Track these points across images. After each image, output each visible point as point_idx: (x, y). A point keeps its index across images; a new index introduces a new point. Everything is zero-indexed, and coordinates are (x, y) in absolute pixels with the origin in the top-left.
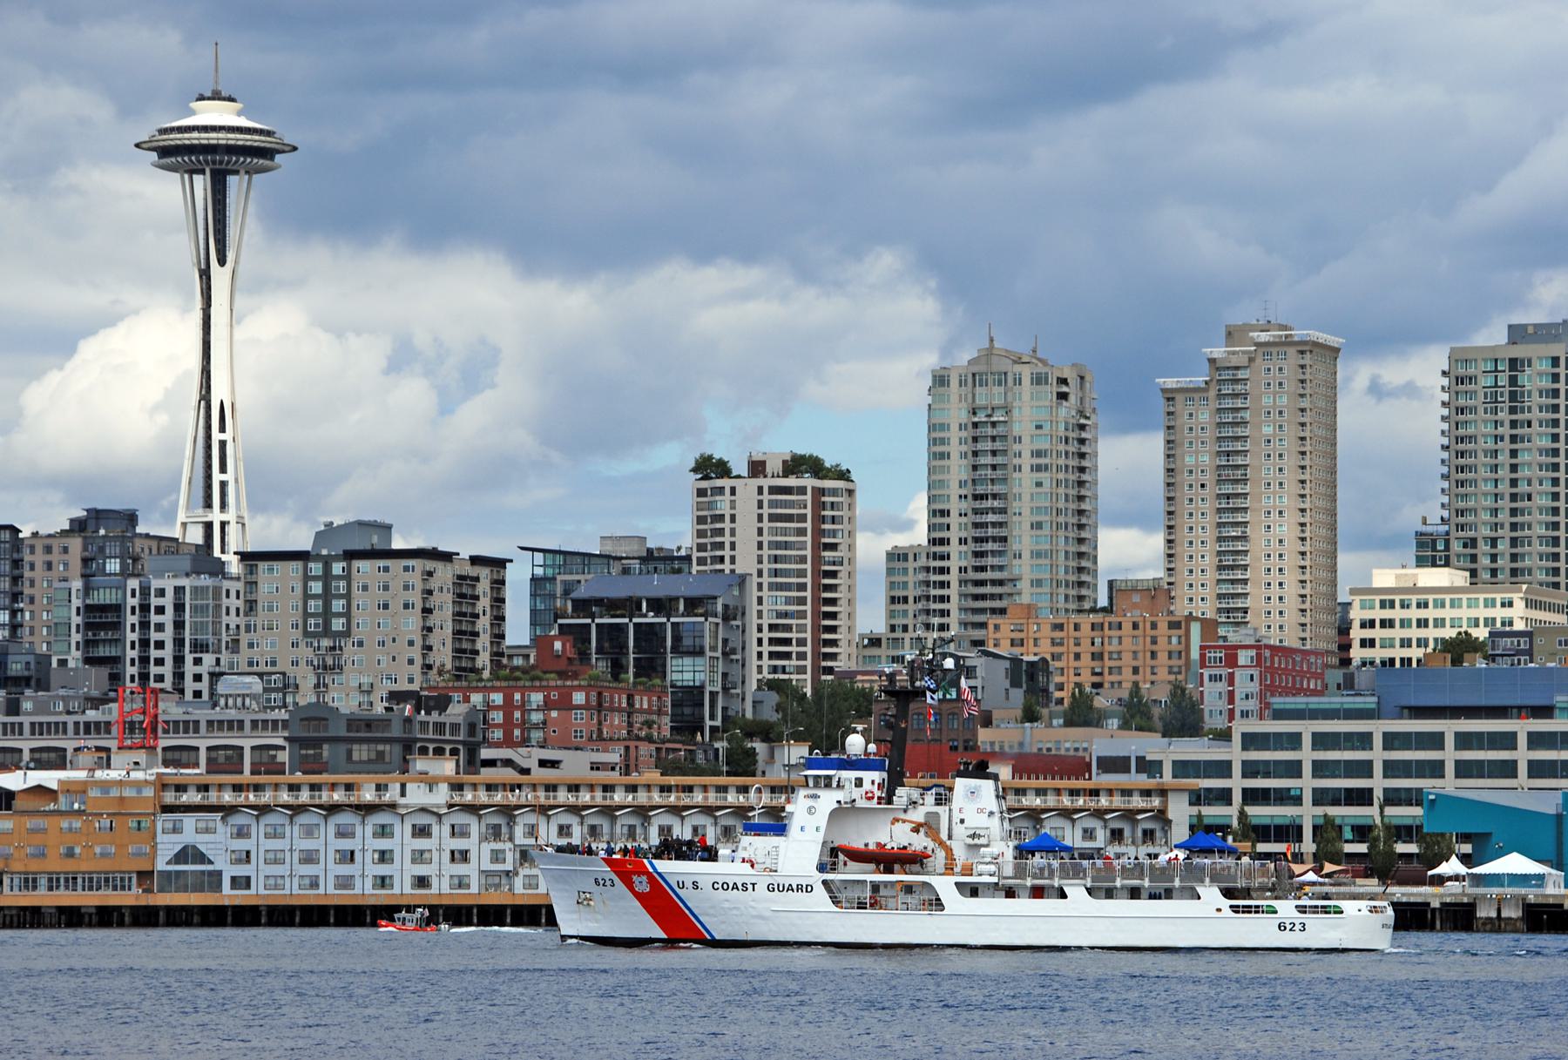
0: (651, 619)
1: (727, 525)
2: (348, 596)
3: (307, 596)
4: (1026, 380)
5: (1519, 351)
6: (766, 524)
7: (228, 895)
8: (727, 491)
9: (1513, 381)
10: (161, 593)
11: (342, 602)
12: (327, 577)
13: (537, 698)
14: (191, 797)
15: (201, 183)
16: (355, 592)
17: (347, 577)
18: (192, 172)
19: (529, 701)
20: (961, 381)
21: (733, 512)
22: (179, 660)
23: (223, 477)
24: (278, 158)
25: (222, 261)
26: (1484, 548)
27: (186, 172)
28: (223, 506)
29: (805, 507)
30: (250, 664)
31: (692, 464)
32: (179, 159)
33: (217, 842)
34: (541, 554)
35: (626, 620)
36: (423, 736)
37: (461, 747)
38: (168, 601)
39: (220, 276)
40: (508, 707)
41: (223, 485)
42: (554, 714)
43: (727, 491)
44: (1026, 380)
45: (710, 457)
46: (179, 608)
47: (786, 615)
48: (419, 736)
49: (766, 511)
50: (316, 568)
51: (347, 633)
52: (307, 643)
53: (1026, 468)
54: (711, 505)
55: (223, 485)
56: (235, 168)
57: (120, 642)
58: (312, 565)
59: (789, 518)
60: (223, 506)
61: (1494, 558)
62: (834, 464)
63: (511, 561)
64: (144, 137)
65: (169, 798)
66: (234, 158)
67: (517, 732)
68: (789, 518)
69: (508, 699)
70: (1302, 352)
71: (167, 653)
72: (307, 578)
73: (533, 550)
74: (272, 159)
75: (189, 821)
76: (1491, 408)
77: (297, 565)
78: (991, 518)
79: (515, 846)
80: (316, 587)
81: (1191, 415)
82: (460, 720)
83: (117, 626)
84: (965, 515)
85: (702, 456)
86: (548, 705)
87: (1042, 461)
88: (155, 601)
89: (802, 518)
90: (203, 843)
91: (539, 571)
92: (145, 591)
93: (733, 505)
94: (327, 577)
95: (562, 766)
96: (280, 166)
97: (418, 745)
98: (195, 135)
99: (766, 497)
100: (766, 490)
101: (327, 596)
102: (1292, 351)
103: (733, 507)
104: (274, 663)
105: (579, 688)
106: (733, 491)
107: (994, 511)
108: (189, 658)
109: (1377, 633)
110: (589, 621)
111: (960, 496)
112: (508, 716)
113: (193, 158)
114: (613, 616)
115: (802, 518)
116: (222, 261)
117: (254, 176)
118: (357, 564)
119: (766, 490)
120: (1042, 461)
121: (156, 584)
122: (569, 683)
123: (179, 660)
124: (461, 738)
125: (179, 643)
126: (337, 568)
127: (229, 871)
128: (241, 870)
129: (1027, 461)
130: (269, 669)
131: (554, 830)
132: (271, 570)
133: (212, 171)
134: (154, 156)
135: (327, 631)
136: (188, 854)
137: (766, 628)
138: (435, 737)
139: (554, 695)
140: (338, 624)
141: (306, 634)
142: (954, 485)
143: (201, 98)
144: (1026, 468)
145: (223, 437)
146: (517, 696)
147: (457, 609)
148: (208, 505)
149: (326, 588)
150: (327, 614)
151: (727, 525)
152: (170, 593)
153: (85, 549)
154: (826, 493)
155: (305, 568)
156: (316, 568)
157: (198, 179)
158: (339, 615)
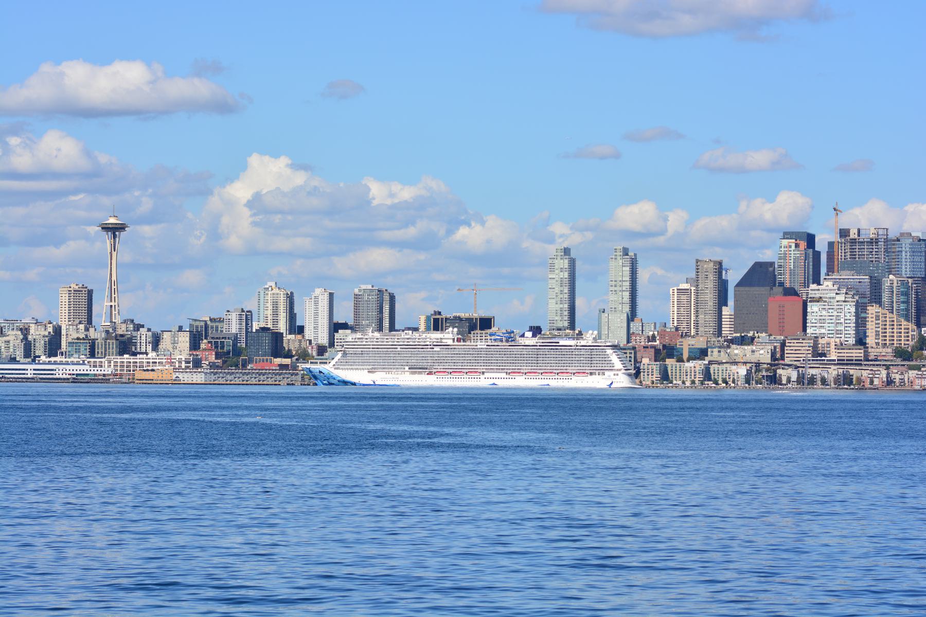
2: (178, 338)
6: (237, 321)
7: (182, 382)
14: (177, 370)
22: (146, 345)
24: (126, 229)
25: (115, 251)
28: (115, 301)
33: (181, 376)
39: (114, 254)
41: (115, 297)
50: (173, 333)
55: (115, 297)
60: (115, 301)
65: (175, 370)
71: (144, 344)
75: (177, 373)
86: (208, 355)
99: (237, 316)
108: (148, 345)
109: (339, 341)
116: (115, 251)
121: (142, 333)
123: (146, 345)
125: (146, 343)
127: (182, 379)
128: (184, 379)
136: (177, 377)
143: (110, 217)
146: (204, 353)
148: (111, 301)
151: (231, 320)
152: (145, 335)
156: (173, 333)
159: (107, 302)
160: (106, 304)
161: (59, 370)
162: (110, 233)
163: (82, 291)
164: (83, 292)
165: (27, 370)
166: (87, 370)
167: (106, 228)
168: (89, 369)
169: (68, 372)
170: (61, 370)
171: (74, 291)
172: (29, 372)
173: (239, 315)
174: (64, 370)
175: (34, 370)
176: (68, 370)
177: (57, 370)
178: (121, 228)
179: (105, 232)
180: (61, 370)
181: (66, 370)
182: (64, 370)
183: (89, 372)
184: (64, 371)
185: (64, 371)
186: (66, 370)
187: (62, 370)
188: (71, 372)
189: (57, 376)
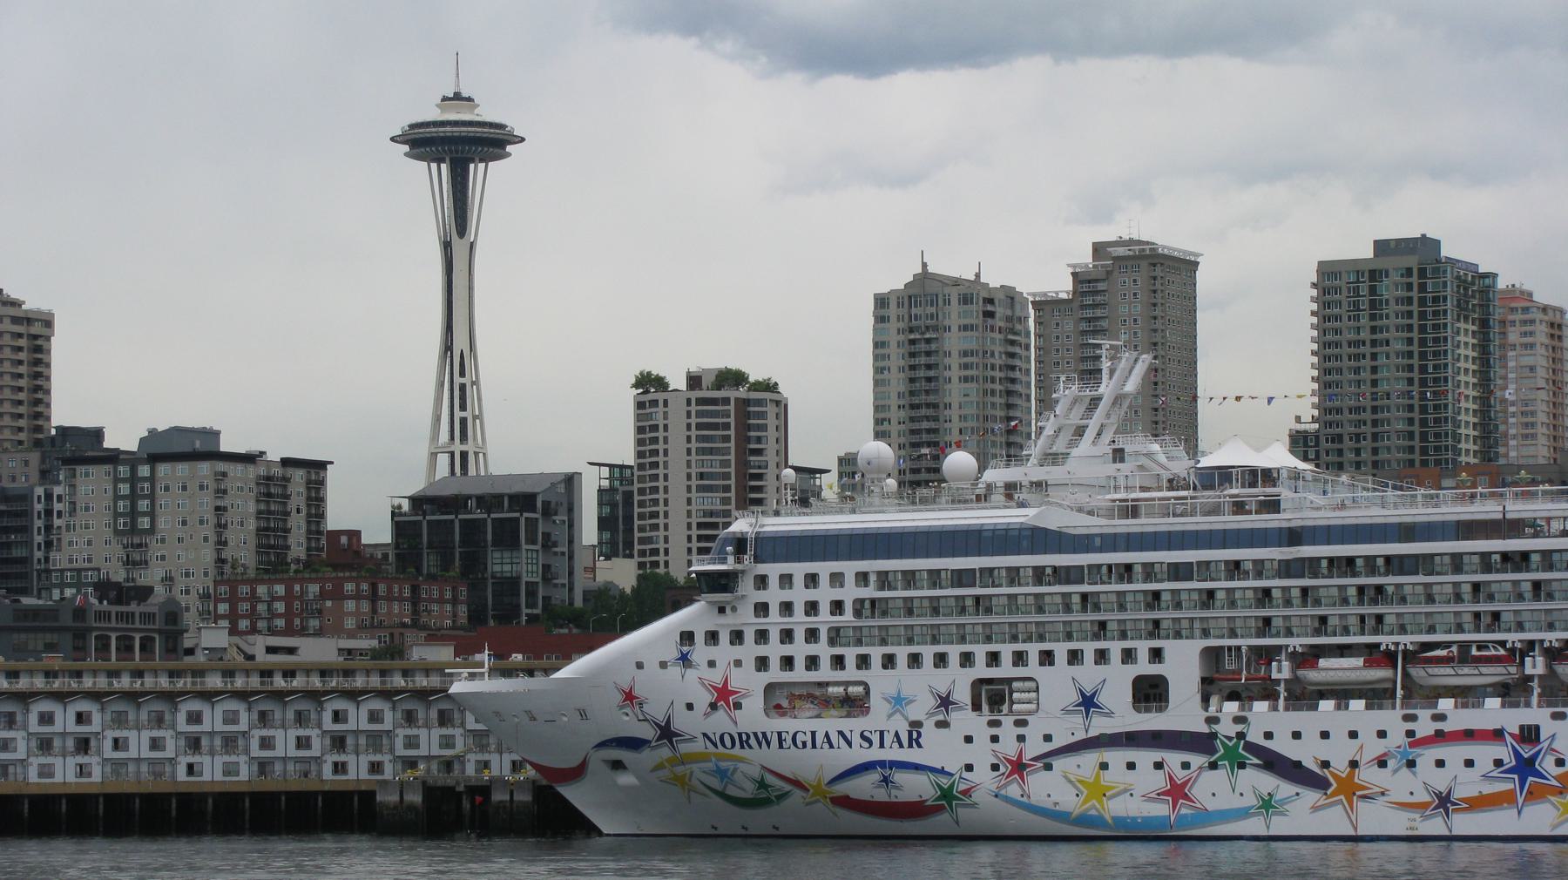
0: (479, 515)
1: (661, 434)
2: (152, 497)
3: (117, 497)
4: (954, 301)
5: (1382, 264)
8: (661, 403)
9: (1373, 290)
11: (146, 502)
12: (133, 479)
13: (314, 589)
16: (159, 492)
17: (152, 479)
18: (439, 161)
19: (307, 592)
20: (898, 303)
21: (665, 422)
23: (463, 414)
24: (509, 148)
26: (1348, 443)
27: (434, 160)
29: (729, 416)
30: (71, 561)
31: (633, 381)
32: (428, 149)
34: (608, 468)
35: (452, 517)
36: (98, 625)
37: (157, 637)
40: (288, 598)
42: (329, 604)
43: (661, 403)
44: (954, 301)
45: (649, 374)
47: (711, 514)
48: (94, 625)
49: (694, 421)
51: (152, 530)
52: (118, 540)
53: (955, 380)
54: (649, 416)
56: (469, 156)
57: (28, 544)
58: (121, 468)
59: (715, 426)
61: (1358, 452)
62: (766, 378)
63: (332, 463)
66: (474, 148)
67: (297, 621)
68: (715, 426)
69: (289, 590)
70: (1154, 265)
72: (117, 480)
73: (600, 465)
74: (504, 149)
76: (1354, 316)
77: (108, 467)
78: (925, 425)
79: (29, 734)
80: (124, 489)
81: (1057, 324)
82: (155, 609)
83: (25, 530)
84: (904, 423)
85: (641, 373)
86: (323, 595)
87: (969, 373)
89: (727, 426)
91: (605, 483)
92: (49, 496)
93: (665, 418)
94: (133, 479)
95: (299, 652)
96: (509, 155)
97: (94, 634)
98: (448, 129)
99: (694, 408)
100: (693, 402)
101: (133, 497)
102: (1144, 264)
103: (665, 418)
104: (90, 560)
105: (350, 579)
106: (666, 403)
107: (928, 418)
110: (420, 518)
111: (899, 407)
112: (289, 607)
113: (433, 149)
114: (443, 514)
115: (727, 426)
117: (490, 164)
118: (163, 469)
119: (693, 402)
120: (969, 373)
122: (341, 575)
124: (157, 627)
126: (144, 471)
129: (955, 373)
130: (86, 565)
131: (71, 718)
132: (87, 475)
133: (451, 160)
134: (406, 148)
135: (133, 529)
137: (694, 526)
138: (143, 626)
139: (328, 586)
140: (144, 522)
141: (117, 532)
142: (894, 396)
144: (955, 380)
145: (463, 380)
146: (297, 588)
147: (263, 507)
149: (133, 489)
150: (133, 513)
151: (661, 434)
153: (43, 461)
154: (752, 403)
155: (115, 470)
156: (123, 470)
157: (444, 166)
158: (144, 514)
162: (434, 166)
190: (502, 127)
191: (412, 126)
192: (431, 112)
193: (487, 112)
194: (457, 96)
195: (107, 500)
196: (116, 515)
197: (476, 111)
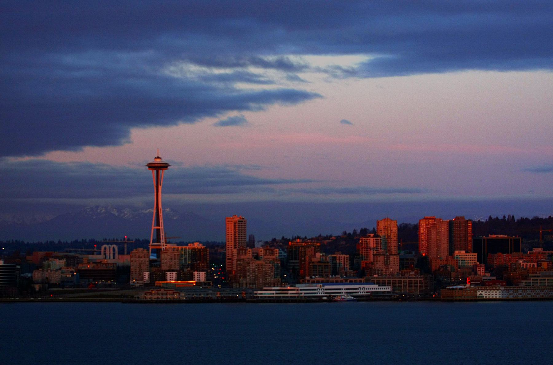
3: (384, 260)
10: (342, 257)
12: (387, 257)
15: (155, 171)
24: (169, 167)
38: (343, 258)
46: (344, 259)
64: (146, 165)
72: (384, 258)
77: (383, 256)
80: (386, 259)
88: (341, 258)
90: (482, 293)
99: (374, 240)
106: (370, 239)
117: (163, 171)
134: (147, 167)
140: (389, 263)
156: (385, 256)
159: (154, 227)
160: (153, 228)
161: (361, 289)
163: (243, 221)
164: (244, 222)
165: (342, 289)
166: (377, 289)
167: (151, 166)
168: (378, 287)
169: (366, 291)
170: (362, 289)
171: (239, 221)
172: (343, 291)
173: (375, 239)
174: (364, 288)
175: (347, 289)
176: (366, 289)
177: (360, 289)
178: (165, 166)
179: (151, 171)
180: (362, 289)
181: (365, 289)
182: (364, 288)
183: (378, 290)
184: (364, 290)
185: (364, 290)
186: (365, 289)
187: (363, 289)
188: (368, 290)
189: (360, 294)
190: (166, 164)
191: (150, 164)
192: (152, 160)
193: (164, 160)
194: (158, 158)
195: (383, 260)
196: (384, 262)
197: (162, 160)
